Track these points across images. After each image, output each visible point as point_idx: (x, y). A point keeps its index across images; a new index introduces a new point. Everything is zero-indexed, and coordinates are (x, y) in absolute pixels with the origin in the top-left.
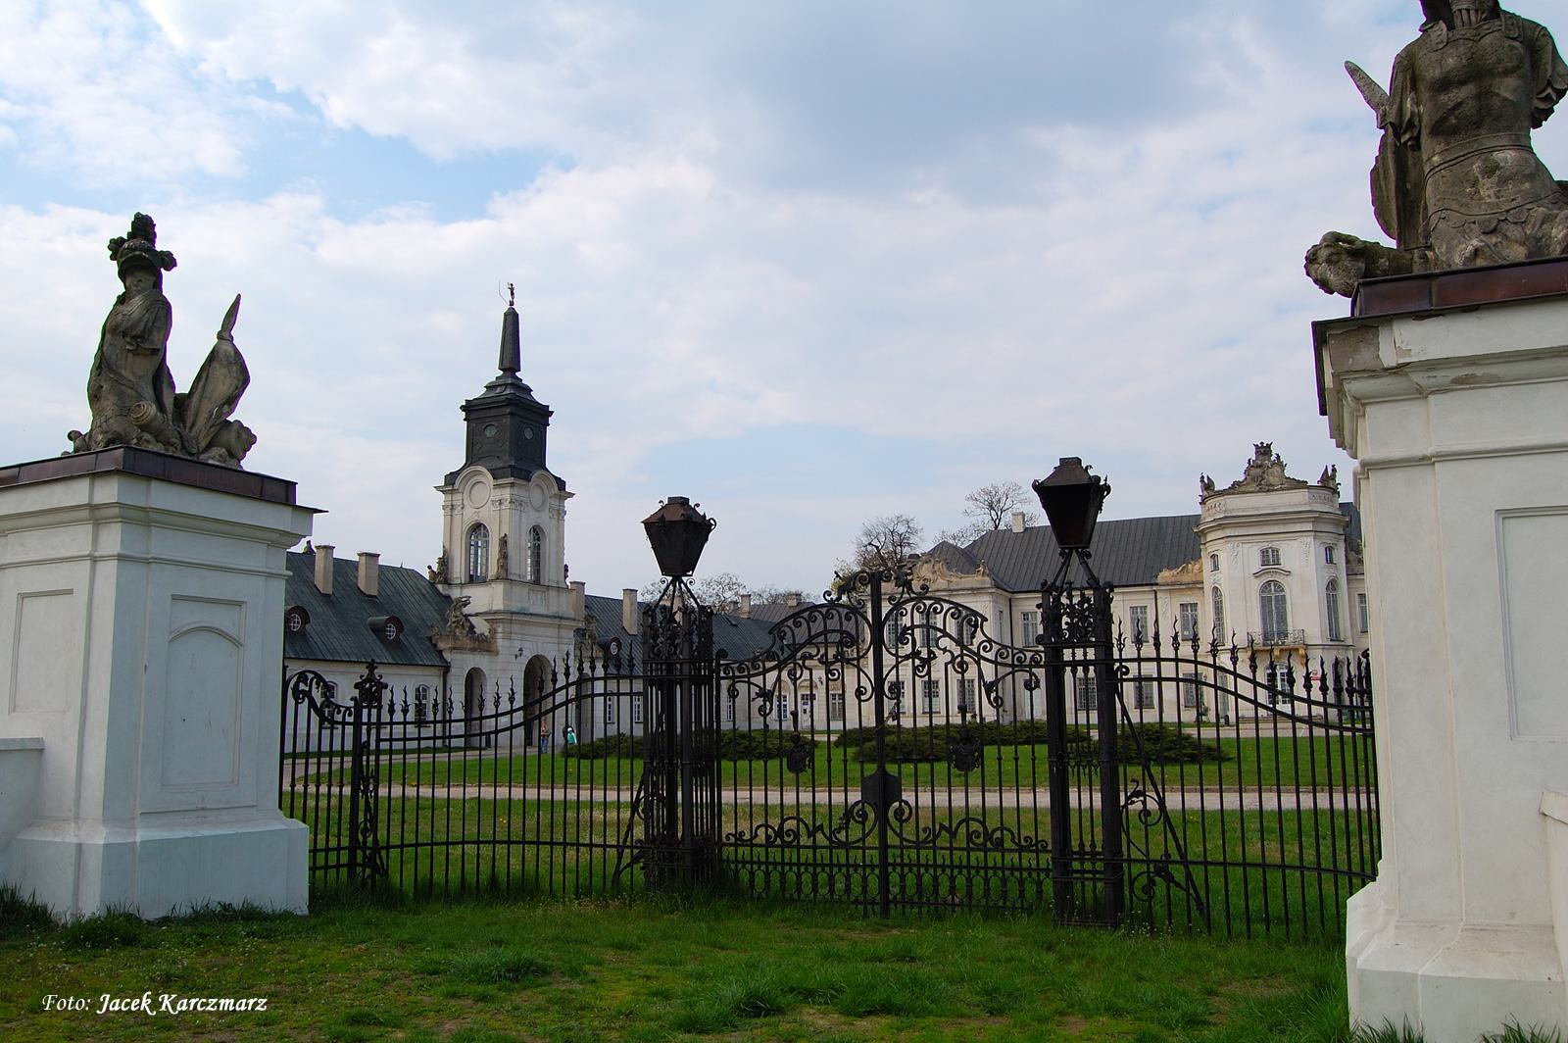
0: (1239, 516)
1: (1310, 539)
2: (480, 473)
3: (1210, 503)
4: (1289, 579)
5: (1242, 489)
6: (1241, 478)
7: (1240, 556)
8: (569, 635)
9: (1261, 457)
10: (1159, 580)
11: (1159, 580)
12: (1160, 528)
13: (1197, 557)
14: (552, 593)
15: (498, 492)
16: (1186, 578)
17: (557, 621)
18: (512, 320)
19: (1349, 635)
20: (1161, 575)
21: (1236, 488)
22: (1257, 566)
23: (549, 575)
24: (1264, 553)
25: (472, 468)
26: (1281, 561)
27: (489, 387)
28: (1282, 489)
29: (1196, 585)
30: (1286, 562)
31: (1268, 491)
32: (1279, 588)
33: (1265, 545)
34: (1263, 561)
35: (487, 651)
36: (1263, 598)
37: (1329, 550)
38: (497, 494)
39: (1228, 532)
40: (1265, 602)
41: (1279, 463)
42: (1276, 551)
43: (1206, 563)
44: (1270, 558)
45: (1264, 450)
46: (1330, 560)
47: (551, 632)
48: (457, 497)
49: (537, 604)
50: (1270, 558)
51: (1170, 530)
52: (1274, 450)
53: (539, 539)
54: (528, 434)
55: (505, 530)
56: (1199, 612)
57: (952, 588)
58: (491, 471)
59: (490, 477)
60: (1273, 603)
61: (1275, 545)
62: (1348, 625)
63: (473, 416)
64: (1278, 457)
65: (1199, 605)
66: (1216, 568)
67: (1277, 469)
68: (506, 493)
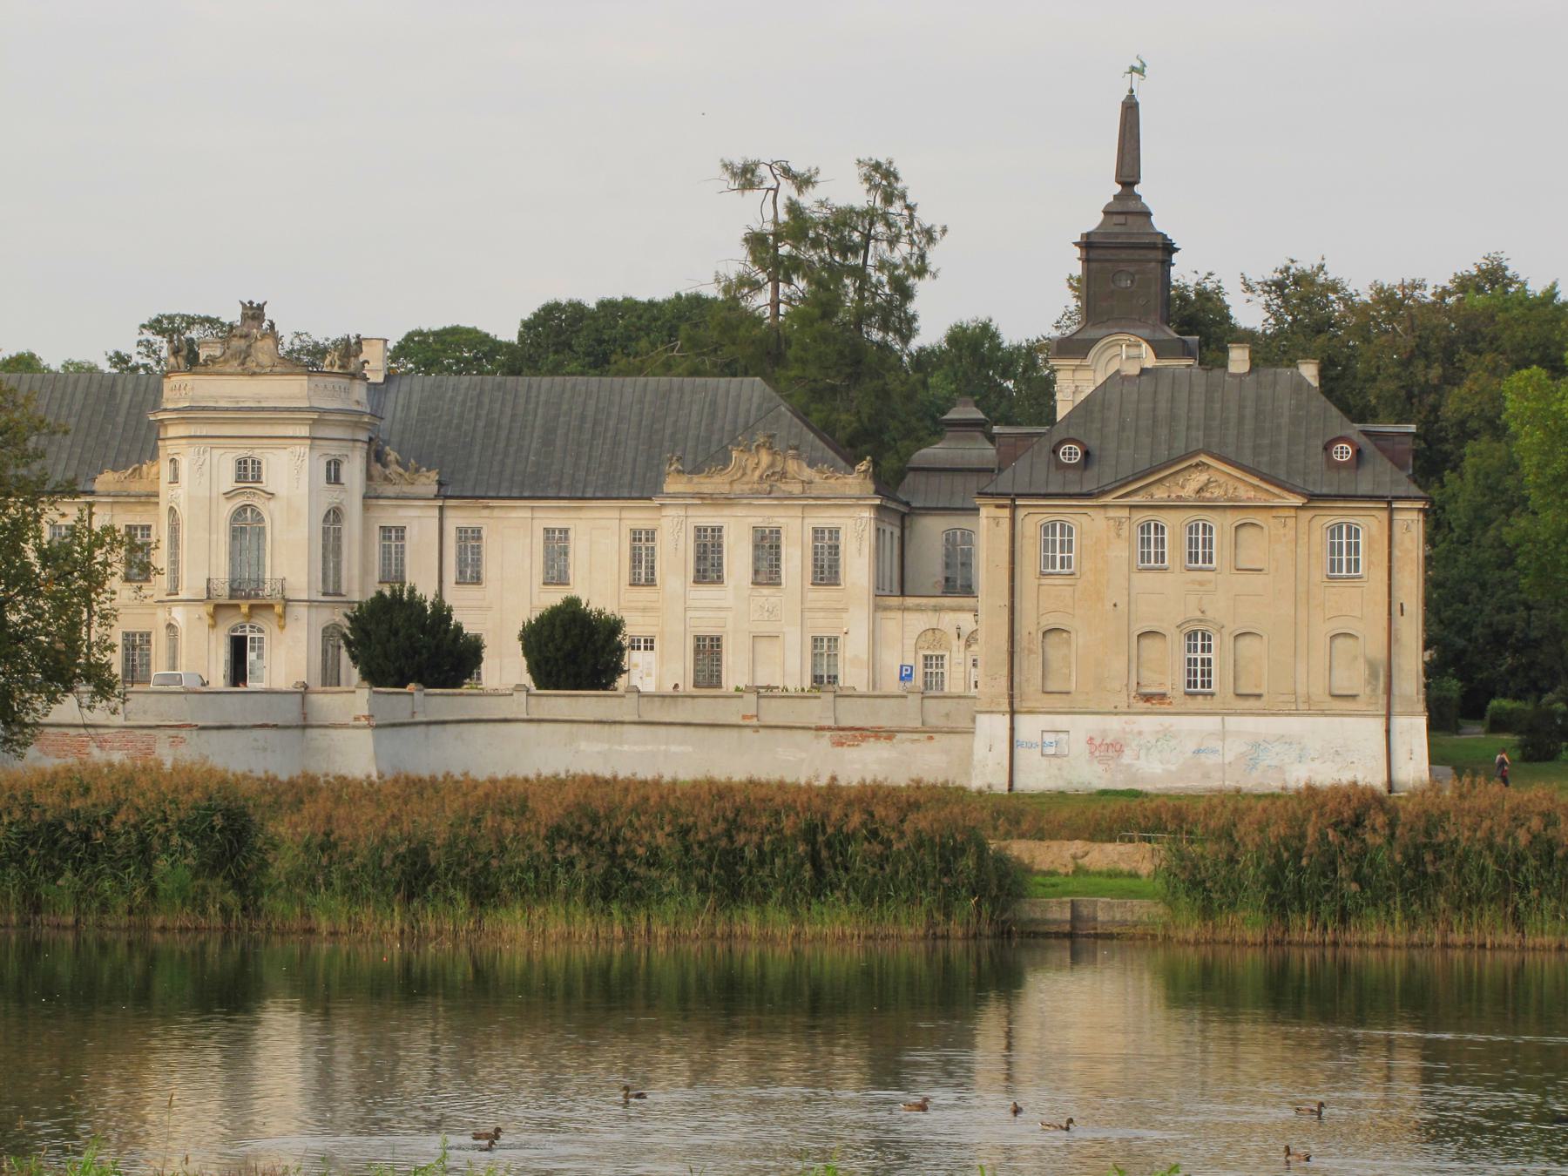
0: (215, 409)
1: (303, 449)
4: (272, 503)
5: (217, 367)
7: (206, 467)
9: (249, 322)
10: (97, 487)
11: (97, 487)
12: (113, 394)
13: (154, 456)
16: (137, 487)
19: (356, 586)
20: (100, 478)
22: (228, 481)
24: (241, 464)
26: (264, 478)
28: (272, 373)
30: (270, 481)
31: (254, 374)
33: (242, 453)
34: (239, 476)
36: (234, 530)
40: (237, 533)
42: (257, 464)
43: (164, 468)
44: (248, 471)
50: (248, 471)
51: (127, 398)
52: (269, 314)
61: (257, 454)
62: (356, 572)
64: (272, 325)
65: (153, 529)
66: (175, 479)
67: (269, 342)
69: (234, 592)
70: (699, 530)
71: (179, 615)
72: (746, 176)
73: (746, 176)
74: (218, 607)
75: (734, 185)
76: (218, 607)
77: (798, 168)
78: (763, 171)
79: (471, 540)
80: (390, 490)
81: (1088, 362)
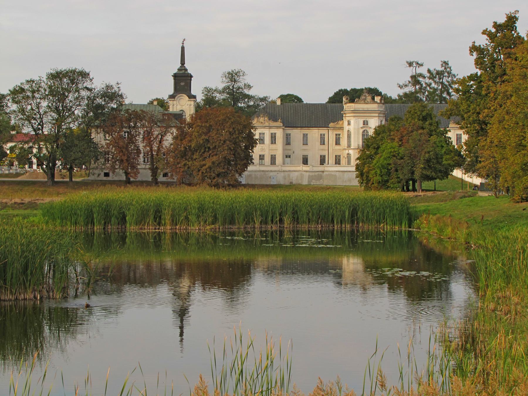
1: (377, 118)
10: (330, 126)
11: (330, 126)
12: (327, 108)
16: (338, 126)
18: (183, 48)
22: (362, 125)
24: (364, 121)
29: (342, 128)
30: (370, 125)
33: (364, 119)
39: (355, 115)
42: (367, 122)
43: (346, 123)
44: (365, 123)
48: (175, 102)
50: (365, 123)
56: (341, 136)
57: (270, 125)
63: (176, 78)
70: (272, 134)
71: (351, 152)
72: (410, 64)
73: (410, 64)
75: (408, 66)
77: (419, 62)
78: (414, 63)
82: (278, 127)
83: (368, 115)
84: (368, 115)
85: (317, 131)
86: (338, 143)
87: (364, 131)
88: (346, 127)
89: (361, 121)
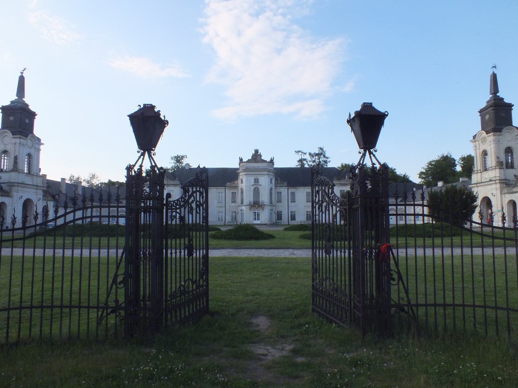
1: (266, 176)
2: (6, 132)
3: (241, 164)
6: (250, 158)
8: (40, 192)
14: (35, 178)
15: (14, 140)
16: (233, 185)
17: (36, 187)
21: (248, 161)
22: (253, 183)
23: (34, 171)
24: (255, 179)
25: (3, 130)
27: (12, 102)
29: (237, 187)
32: (258, 189)
33: (255, 177)
35: (8, 196)
37: (271, 180)
38: (14, 141)
41: (260, 156)
42: (258, 179)
43: (240, 181)
44: (256, 181)
45: (257, 151)
46: (271, 182)
47: (35, 191)
49: (28, 180)
50: (256, 181)
53: (30, 158)
54: (27, 121)
55: (17, 154)
58: (12, 132)
59: (11, 134)
60: (256, 192)
61: (258, 177)
66: (242, 182)
68: (18, 141)
69: (254, 203)
71: (243, 208)
74: (252, 206)
76: (252, 206)
79: (293, 194)
80: (279, 185)
81: (502, 133)
82: (175, 185)
83: (258, 173)
84: (258, 173)
85: (215, 189)
86: (234, 201)
87: (255, 189)
88: (240, 186)
89: (252, 179)
